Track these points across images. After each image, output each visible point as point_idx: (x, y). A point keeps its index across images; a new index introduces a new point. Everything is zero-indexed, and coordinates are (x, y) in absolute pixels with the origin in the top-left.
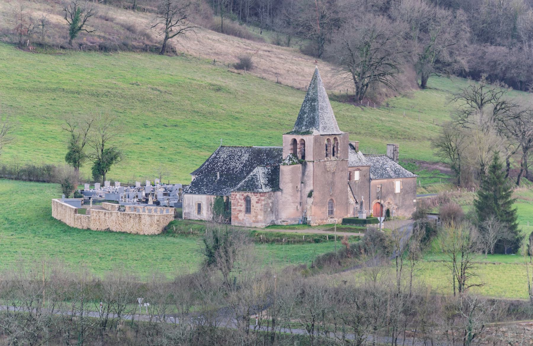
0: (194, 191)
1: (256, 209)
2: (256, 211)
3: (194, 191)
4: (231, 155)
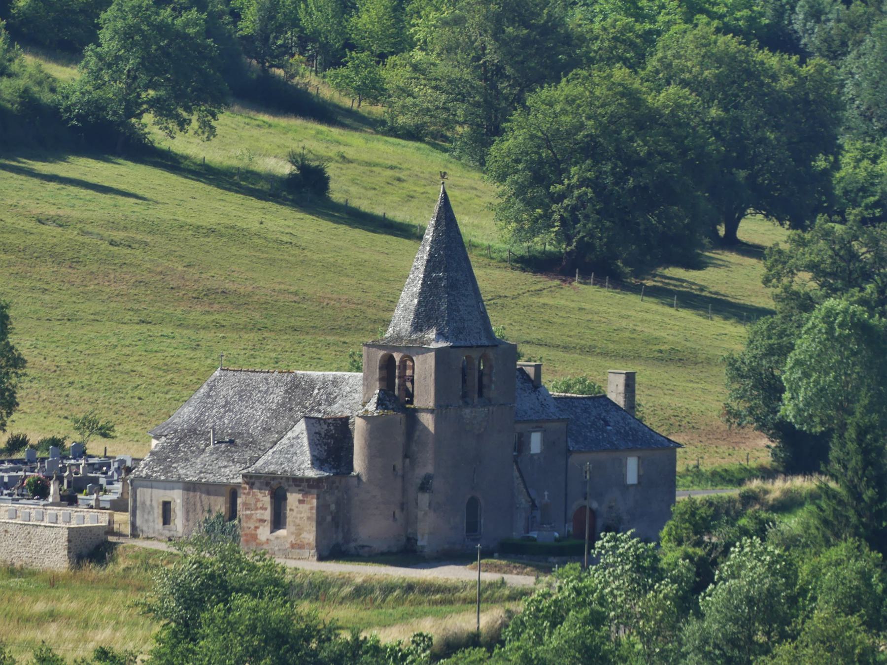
0: (156, 472)
1: (299, 516)
2: (298, 521)
3: (156, 472)
4: (242, 391)
